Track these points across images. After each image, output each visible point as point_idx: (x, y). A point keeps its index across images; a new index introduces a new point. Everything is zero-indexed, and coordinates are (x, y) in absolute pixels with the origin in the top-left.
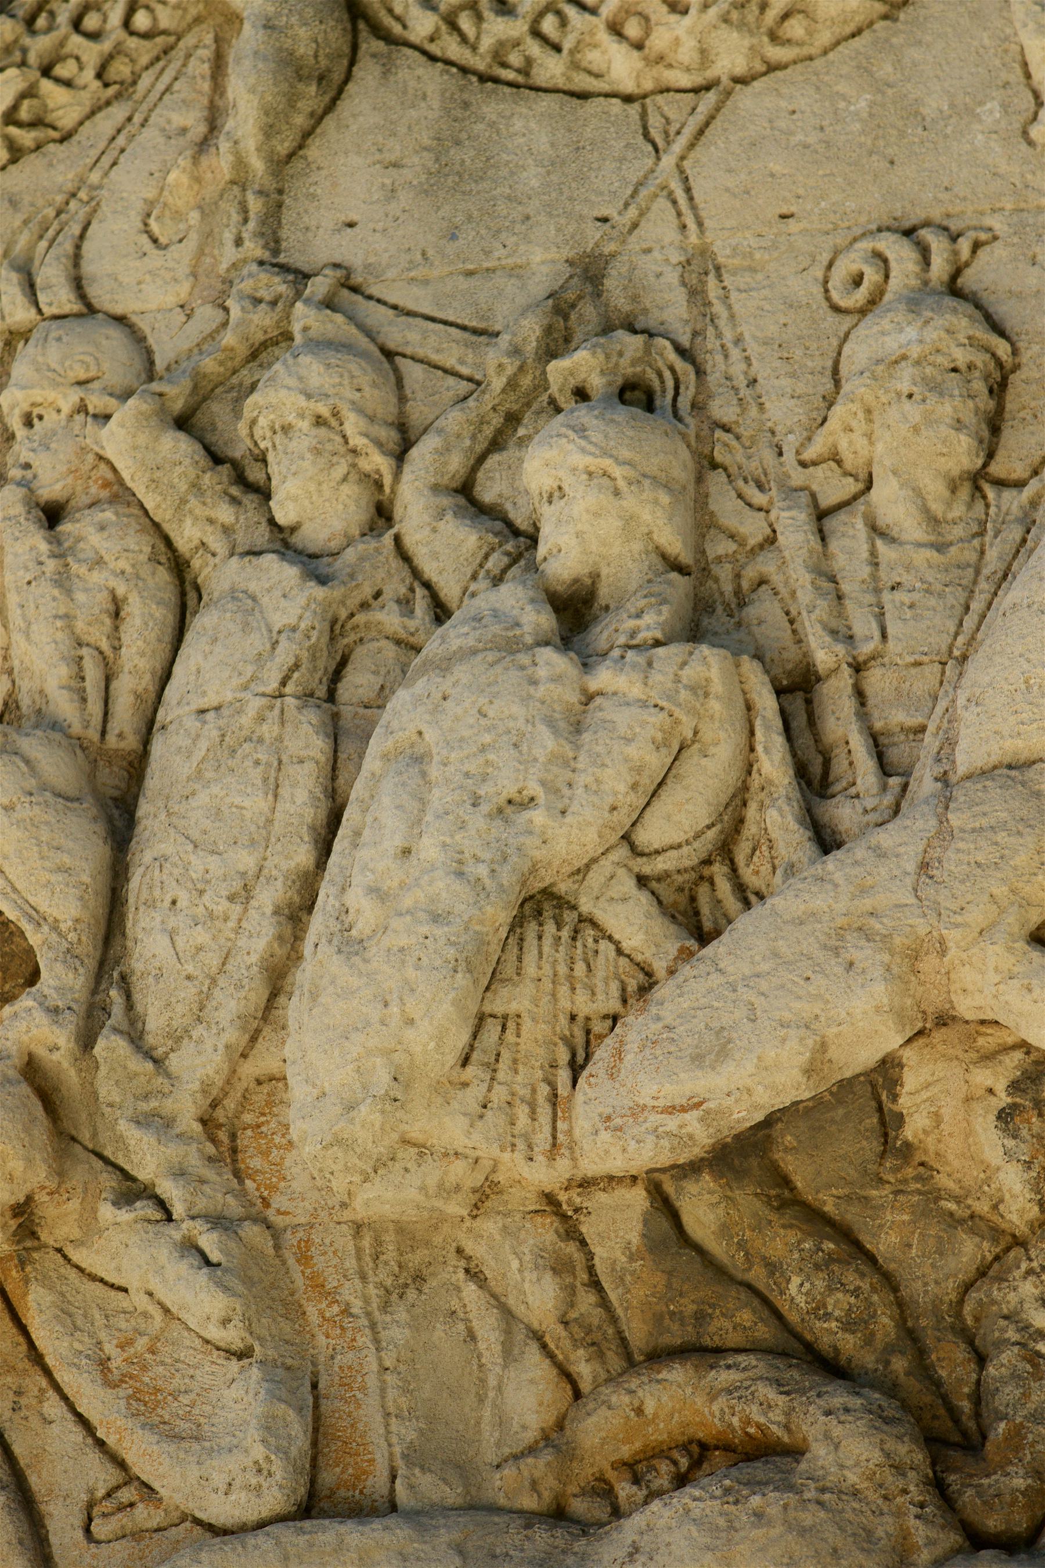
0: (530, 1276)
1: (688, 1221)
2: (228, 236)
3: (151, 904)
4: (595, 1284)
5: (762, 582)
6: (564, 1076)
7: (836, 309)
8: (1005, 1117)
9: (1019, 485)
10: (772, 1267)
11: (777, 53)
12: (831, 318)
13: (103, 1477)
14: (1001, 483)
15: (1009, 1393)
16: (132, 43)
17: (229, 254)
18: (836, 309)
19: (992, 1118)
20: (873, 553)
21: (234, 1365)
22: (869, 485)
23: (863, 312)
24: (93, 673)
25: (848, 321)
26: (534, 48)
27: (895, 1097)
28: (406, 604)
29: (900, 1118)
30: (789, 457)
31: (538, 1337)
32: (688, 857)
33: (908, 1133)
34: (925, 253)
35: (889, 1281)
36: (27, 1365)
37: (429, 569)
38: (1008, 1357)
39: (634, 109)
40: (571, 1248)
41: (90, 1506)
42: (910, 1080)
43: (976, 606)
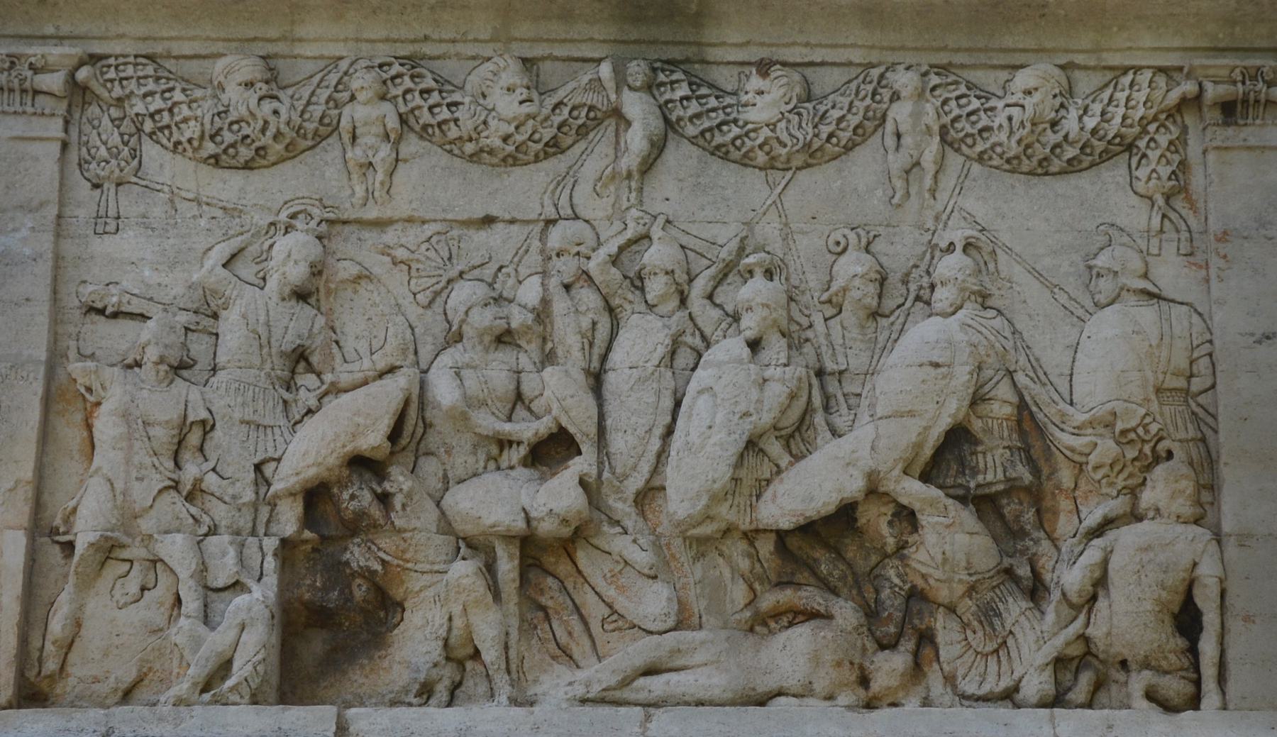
0: (740, 557)
1: (788, 544)
2: (625, 199)
3: (617, 430)
4: (759, 560)
5: (807, 340)
6: (754, 498)
7: (830, 251)
8: (890, 523)
9: (888, 316)
10: (815, 560)
11: (810, 161)
12: (829, 256)
13: (607, 611)
14: (882, 316)
15: (888, 603)
16: (589, 122)
17: (625, 205)
18: (830, 251)
19: (886, 524)
20: (844, 336)
21: (651, 581)
22: (840, 312)
23: (840, 254)
24: (587, 347)
25: (834, 257)
26: (732, 149)
27: (854, 513)
28: (693, 334)
29: (856, 520)
30: (815, 299)
31: (742, 576)
32: (789, 431)
33: (859, 525)
34: (859, 236)
35: (850, 565)
36: (576, 574)
37: (700, 324)
38: (888, 591)
39: (763, 173)
40: (753, 551)
41: (603, 619)
42: (860, 509)
43: (876, 357)
